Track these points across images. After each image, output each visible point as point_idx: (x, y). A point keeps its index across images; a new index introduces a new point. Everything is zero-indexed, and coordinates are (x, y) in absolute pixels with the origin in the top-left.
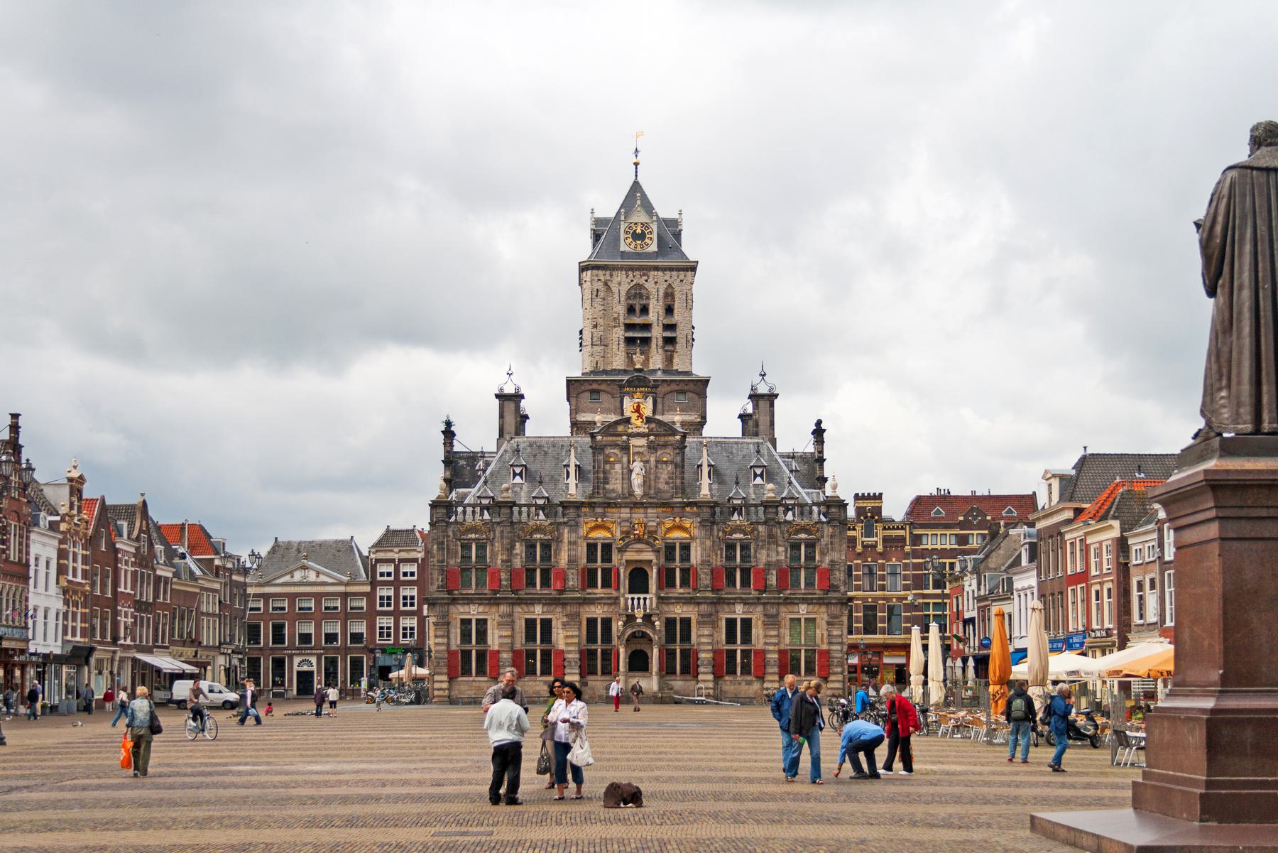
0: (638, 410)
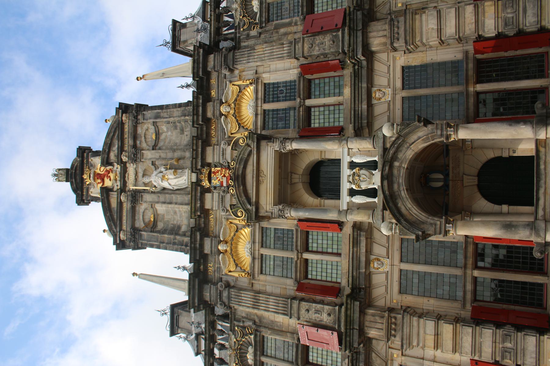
0: (101, 177)
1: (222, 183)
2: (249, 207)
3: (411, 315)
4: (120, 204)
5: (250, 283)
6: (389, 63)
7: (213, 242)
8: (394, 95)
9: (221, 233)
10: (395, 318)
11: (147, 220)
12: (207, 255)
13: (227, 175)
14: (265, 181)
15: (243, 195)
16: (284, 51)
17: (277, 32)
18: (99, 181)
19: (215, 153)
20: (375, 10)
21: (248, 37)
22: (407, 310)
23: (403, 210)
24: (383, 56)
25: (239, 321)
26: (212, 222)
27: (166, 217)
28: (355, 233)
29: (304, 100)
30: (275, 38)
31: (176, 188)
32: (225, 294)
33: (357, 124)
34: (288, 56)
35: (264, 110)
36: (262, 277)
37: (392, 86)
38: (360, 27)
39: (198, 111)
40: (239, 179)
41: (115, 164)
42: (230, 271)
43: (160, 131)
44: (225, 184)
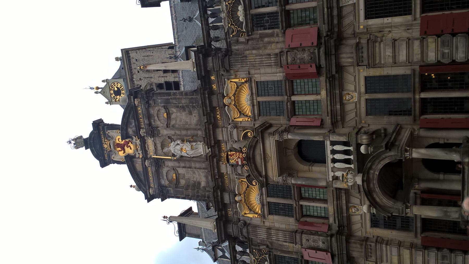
1: (237, 162)
2: (261, 178)
3: (381, 243)
4: (145, 169)
5: (261, 221)
6: (355, 74)
7: (231, 195)
8: (360, 97)
9: (236, 189)
10: (371, 246)
11: (170, 178)
12: (226, 204)
13: (241, 156)
14: (270, 161)
15: (255, 171)
16: (271, 60)
17: (262, 41)
18: (120, 149)
19: (224, 134)
20: (342, 30)
21: (237, 42)
22: (379, 241)
23: (378, 200)
24: (351, 69)
25: (256, 246)
26: (227, 181)
27: (186, 175)
28: (338, 192)
29: (290, 97)
30: (261, 45)
31: (192, 156)
32: (245, 230)
33: (333, 120)
34: (275, 65)
35: (259, 102)
36: (271, 217)
37: (358, 91)
38: (333, 52)
39: (205, 103)
40: (250, 159)
41: (134, 137)
42: (246, 214)
43: (171, 112)
44: (240, 163)
